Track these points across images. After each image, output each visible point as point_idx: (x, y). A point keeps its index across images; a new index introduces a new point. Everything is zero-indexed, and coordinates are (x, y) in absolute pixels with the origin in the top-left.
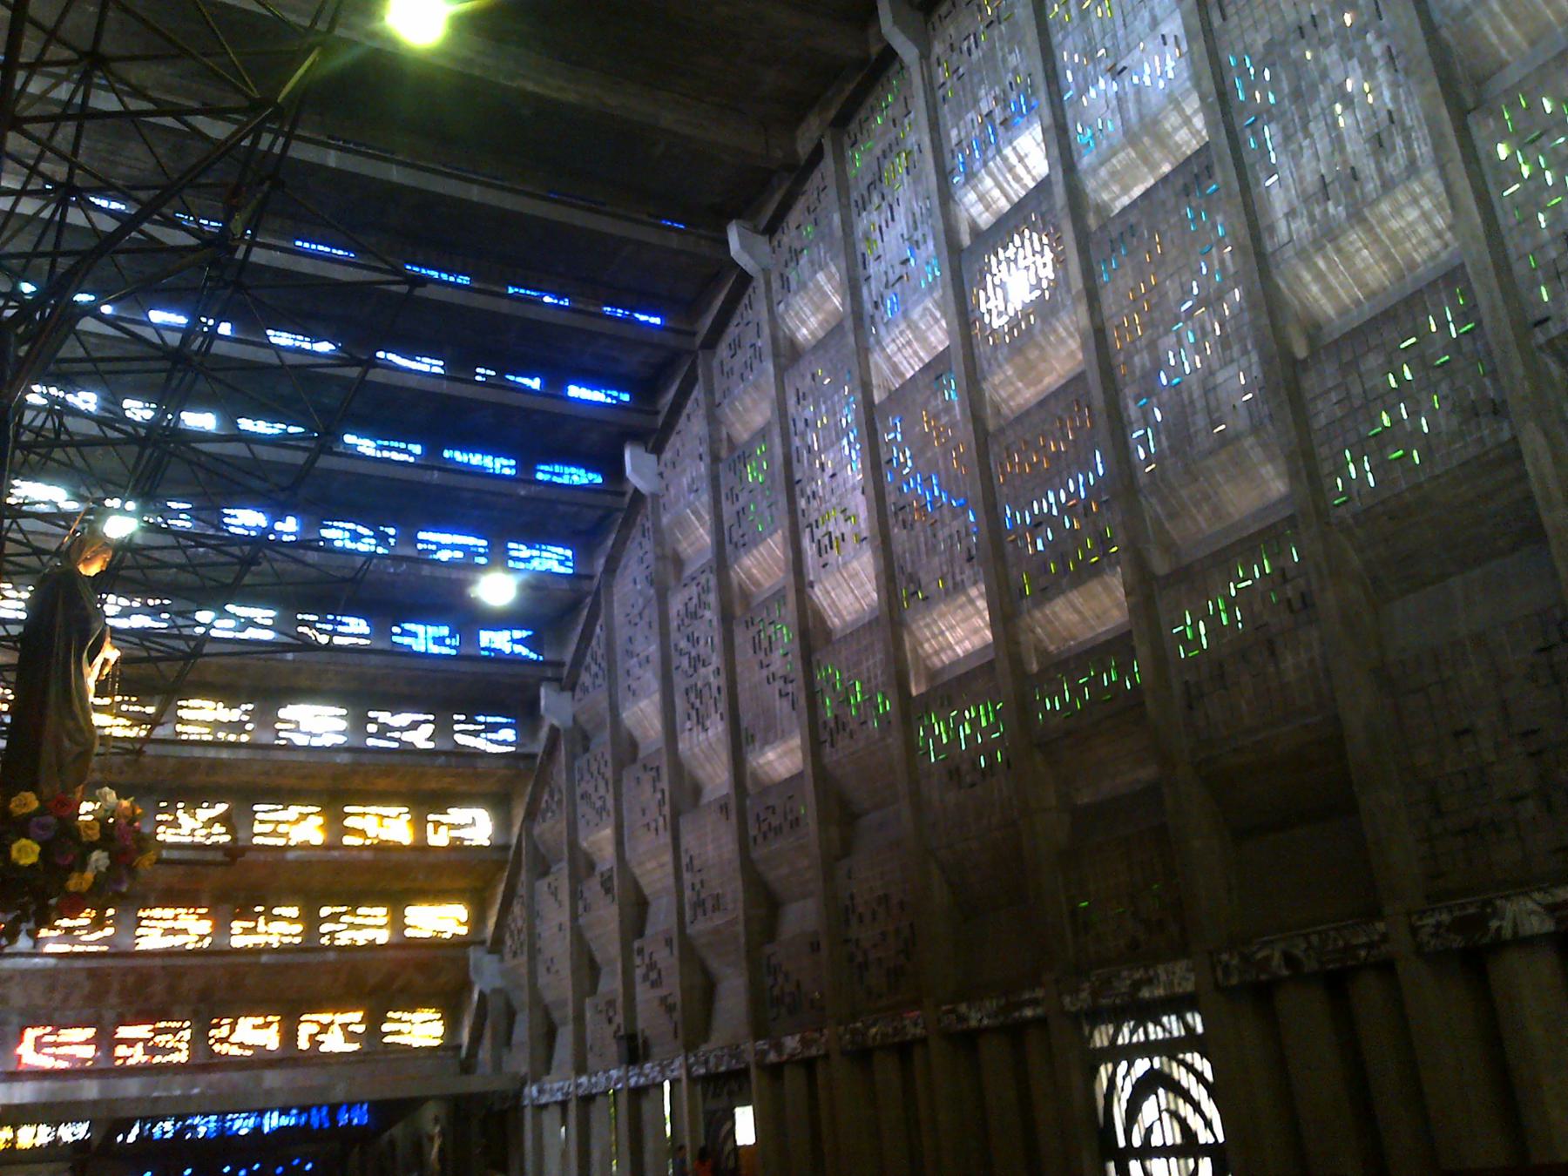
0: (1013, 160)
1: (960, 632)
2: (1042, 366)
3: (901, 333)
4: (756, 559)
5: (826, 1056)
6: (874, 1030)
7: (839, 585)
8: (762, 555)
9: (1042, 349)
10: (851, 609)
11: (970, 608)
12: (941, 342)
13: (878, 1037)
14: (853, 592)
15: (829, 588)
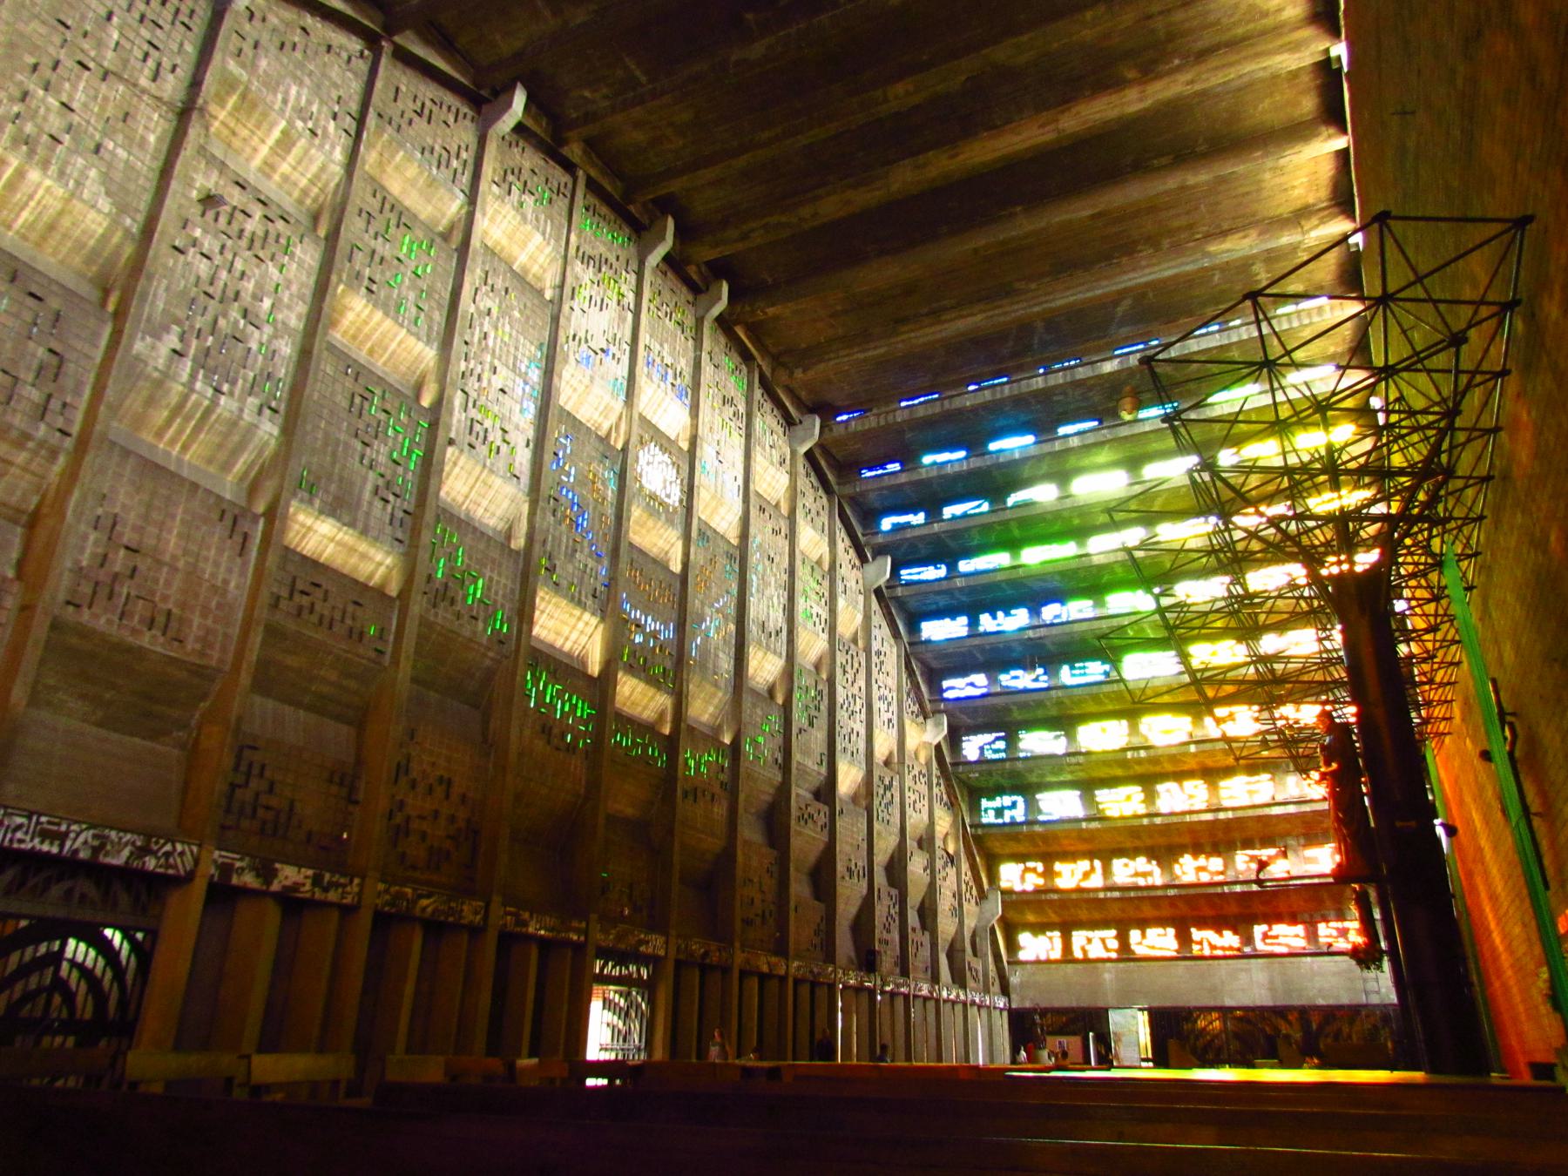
1: (551, 624)
2: (644, 531)
4: (370, 316)
5: (348, 911)
6: (424, 902)
8: (379, 324)
10: (453, 494)
11: (573, 621)
13: (430, 910)
14: (472, 488)
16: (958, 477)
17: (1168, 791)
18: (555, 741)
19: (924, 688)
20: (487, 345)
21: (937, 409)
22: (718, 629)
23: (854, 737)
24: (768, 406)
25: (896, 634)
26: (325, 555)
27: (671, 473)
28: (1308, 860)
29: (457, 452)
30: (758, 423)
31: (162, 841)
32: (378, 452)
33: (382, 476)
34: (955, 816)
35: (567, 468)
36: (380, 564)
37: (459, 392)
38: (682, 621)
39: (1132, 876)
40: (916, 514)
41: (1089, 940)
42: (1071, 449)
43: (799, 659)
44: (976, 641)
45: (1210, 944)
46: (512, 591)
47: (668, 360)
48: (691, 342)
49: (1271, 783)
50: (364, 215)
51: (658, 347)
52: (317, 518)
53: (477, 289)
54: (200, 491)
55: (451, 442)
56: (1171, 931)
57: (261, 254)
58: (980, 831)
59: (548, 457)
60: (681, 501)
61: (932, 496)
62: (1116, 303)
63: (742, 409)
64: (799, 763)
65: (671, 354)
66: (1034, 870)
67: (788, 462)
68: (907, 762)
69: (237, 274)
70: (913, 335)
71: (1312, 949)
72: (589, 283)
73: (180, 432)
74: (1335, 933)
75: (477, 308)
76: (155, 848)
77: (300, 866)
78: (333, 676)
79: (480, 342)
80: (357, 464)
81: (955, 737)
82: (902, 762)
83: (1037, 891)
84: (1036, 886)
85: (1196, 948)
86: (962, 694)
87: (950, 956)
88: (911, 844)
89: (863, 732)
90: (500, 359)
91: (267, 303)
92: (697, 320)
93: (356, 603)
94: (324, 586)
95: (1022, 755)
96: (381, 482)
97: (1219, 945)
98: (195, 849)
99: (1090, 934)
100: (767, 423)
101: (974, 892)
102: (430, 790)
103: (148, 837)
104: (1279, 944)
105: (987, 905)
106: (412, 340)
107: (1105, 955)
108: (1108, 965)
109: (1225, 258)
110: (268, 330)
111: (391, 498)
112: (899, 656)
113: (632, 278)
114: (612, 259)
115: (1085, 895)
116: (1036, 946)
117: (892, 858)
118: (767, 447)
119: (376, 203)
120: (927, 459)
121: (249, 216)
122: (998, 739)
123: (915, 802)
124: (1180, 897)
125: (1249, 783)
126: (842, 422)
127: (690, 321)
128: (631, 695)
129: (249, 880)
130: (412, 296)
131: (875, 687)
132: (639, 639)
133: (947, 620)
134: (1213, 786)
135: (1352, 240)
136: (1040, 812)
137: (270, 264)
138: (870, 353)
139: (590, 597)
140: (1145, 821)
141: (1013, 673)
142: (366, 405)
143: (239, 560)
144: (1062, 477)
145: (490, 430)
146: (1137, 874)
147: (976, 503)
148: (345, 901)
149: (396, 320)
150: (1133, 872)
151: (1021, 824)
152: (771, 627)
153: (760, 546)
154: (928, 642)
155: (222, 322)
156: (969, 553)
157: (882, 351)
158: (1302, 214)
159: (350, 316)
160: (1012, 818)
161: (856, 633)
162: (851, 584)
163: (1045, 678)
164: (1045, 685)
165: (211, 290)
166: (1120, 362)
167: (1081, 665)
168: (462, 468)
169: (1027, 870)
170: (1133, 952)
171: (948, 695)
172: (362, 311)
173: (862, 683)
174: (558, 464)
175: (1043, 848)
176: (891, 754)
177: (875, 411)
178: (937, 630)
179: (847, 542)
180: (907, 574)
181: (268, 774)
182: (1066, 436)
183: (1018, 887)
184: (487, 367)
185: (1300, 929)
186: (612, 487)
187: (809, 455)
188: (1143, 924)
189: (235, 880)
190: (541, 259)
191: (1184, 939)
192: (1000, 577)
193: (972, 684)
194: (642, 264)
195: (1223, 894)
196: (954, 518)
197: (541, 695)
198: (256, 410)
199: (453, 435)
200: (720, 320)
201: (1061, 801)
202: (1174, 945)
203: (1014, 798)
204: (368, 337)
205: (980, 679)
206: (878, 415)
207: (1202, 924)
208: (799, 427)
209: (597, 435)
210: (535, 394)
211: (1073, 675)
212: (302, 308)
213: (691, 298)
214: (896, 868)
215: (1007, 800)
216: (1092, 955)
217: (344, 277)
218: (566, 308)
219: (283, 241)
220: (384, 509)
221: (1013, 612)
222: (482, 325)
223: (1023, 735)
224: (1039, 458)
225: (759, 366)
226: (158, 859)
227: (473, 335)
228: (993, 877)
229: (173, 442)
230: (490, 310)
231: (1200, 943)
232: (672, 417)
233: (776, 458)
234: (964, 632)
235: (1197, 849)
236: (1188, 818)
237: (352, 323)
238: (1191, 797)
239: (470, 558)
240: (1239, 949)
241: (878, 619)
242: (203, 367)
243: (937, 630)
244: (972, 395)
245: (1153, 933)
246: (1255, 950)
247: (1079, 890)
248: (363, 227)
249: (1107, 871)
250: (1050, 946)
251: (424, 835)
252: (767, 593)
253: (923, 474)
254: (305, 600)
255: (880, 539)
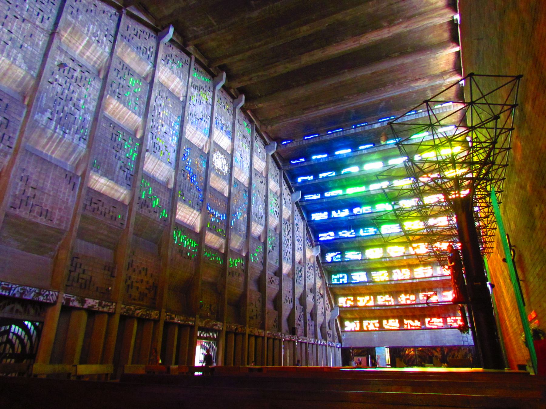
0: (222, 138)
2: (215, 182)
3: (193, 130)
4: (118, 107)
5: (111, 315)
6: (138, 311)
7: (154, 162)
8: (122, 109)
9: (219, 180)
10: (148, 168)
11: (190, 213)
12: (193, 142)
13: (140, 314)
15: (151, 158)
16: (324, 163)
17: (396, 272)
18: (184, 255)
19: (312, 237)
20: (160, 117)
21: (318, 140)
22: (241, 216)
23: (288, 254)
24: (258, 138)
25: (303, 218)
26: (103, 190)
27: (225, 162)
28: (444, 296)
29: (149, 154)
30: (255, 145)
31: (45, 291)
32: (121, 154)
33: (123, 163)
34: (323, 281)
35: (188, 160)
36: (122, 193)
37: (150, 133)
38: (228, 213)
39: (383, 302)
40: (310, 176)
41: (369, 324)
42: (363, 154)
43: (269, 227)
44: (331, 221)
45: (410, 325)
46: (169, 203)
47: (224, 122)
48: (232, 116)
49: (432, 270)
50: (117, 71)
51: (220, 118)
52: (100, 177)
53: (156, 97)
54: (58, 168)
55: (147, 151)
56: (397, 321)
57: (80, 84)
58: (332, 286)
59: (181, 156)
60: (228, 171)
61: (315, 169)
62: (379, 104)
63: (249, 139)
64: (269, 263)
65: (225, 120)
66: (350, 300)
67: (265, 158)
68: (307, 262)
69: (71, 91)
70: (309, 114)
71: (445, 326)
72: (196, 95)
73: (51, 147)
74: (453, 321)
75: (157, 104)
76: (43, 293)
77: (94, 299)
78: (106, 233)
79: (157, 116)
80: (114, 158)
81: (323, 254)
82: (305, 262)
83: (351, 307)
84: (351, 305)
85: (405, 326)
86: (326, 239)
87: (321, 329)
88: (308, 291)
89: (291, 252)
90: (164, 122)
91: (82, 102)
92: (234, 108)
93: (114, 207)
94: (102, 201)
95: (346, 260)
96: (122, 165)
97: (413, 325)
98: (57, 293)
99: (369, 322)
100: (258, 144)
101: (330, 307)
102: (140, 272)
103: (40, 289)
104: (434, 325)
105: (334, 312)
106: (133, 115)
107: (374, 329)
108: (376, 332)
109: (417, 88)
110: (82, 111)
111: (126, 170)
112: (304, 226)
113: (211, 94)
114: (204, 87)
115: (368, 308)
116: (350, 326)
117: (301, 295)
118: (258, 153)
119: (120, 67)
120: (314, 157)
121: (75, 71)
122: (338, 254)
123: (309, 276)
124: (400, 309)
125: (424, 270)
126: (284, 144)
127: (231, 109)
128: (211, 239)
129: (76, 304)
130: (133, 99)
131: (295, 236)
132: (213, 220)
133: (321, 213)
134: (412, 271)
135: (461, 83)
136: (353, 280)
137: (83, 88)
138: (294, 121)
139: (196, 205)
140: (389, 283)
141: (343, 231)
142: (117, 138)
143: (72, 192)
144: (360, 164)
145: (161, 146)
146: (385, 301)
147: (331, 173)
148: (110, 311)
149: (127, 107)
150: (384, 300)
151: (346, 283)
152: (259, 215)
153: (256, 187)
154: (314, 220)
155: (66, 108)
156: (328, 190)
157: (299, 119)
158: (443, 74)
159: (112, 106)
160: (343, 282)
161: (289, 218)
162: (287, 201)
163: (354, 233)
164: (354, 236)
165: (62, 97)
166: (381, 124)
167: (367, 229)
168: (151, 160)
169: (347, 299)
170: (384, 328)
171: (321, 239)
172: (115, 105)
173: (291, 235)
174: (185, 158)
175: (353, 292)
176: (301, 259)
177: (296, 140)
178: (317, 217)
179: (286, 186)
180: (307, 197)
181: (82, 267)
182: (362, 150)
183: (345, 306)
184: (160, 124)
185: (441, 320)
186: (204, 166)
187: (273, 156)
188: (387, 318)
189: (71, 304)
190: (179, 87)
191: (401, 323)
192: (339, 198)
193: (329, 235)
194: (214, 88)
195: (415, 308)
196: (323, 178)
197: (179, 239)
198: (78, 139)
199: (148, 148)
200: (242, 108)
201: (360, 276)
202: (398, 325)
203: (344, 275)
204: (118, 114)
205: (332, 234)
206: (297, 142)
207: (408, 318)
208: (269, 146)
209: (199, 148)
210: (177, 134)
211: (364, 232)
212: (95, 104)
213: (232, 101)
214: (303, 299)
215: (341, 276)
216: (370, 329)
217: (109, 92)
218: (188, 104)
219: (87, 80)
220: (124, 174)
221: (343, 210)
222: (158, 110)
223: (346, 253)
224: (352, 157)
225: (255, 125)
226: (44, 297)
227: (155, 113)
228: (336, 302)
229: (48, 150)
230: (161, 104)
231: (407, 324)
232: (225, 142)
233: (261, 157)
234: (326, 217)
235: (406, 292)
236: (403, 282)
237: (112, 109)
238: (404, 275)
239: (154, 191)
240: (420, 327)
241: (297, 213)
242: (59, 124)
243: (317, 217)
244: (329, 136)
245: (391, 321)
246: (426, 327)
247: (366, 306)
248: (116, 75)
249: (375, 300)
250: (355, 326)
251: (138, 288)
252: (258, 203)
253: (312, 162)
254: (96, 206)
255: (297, 185)
